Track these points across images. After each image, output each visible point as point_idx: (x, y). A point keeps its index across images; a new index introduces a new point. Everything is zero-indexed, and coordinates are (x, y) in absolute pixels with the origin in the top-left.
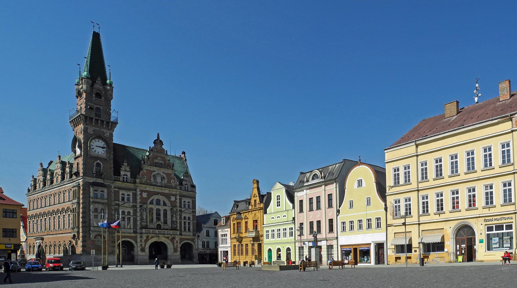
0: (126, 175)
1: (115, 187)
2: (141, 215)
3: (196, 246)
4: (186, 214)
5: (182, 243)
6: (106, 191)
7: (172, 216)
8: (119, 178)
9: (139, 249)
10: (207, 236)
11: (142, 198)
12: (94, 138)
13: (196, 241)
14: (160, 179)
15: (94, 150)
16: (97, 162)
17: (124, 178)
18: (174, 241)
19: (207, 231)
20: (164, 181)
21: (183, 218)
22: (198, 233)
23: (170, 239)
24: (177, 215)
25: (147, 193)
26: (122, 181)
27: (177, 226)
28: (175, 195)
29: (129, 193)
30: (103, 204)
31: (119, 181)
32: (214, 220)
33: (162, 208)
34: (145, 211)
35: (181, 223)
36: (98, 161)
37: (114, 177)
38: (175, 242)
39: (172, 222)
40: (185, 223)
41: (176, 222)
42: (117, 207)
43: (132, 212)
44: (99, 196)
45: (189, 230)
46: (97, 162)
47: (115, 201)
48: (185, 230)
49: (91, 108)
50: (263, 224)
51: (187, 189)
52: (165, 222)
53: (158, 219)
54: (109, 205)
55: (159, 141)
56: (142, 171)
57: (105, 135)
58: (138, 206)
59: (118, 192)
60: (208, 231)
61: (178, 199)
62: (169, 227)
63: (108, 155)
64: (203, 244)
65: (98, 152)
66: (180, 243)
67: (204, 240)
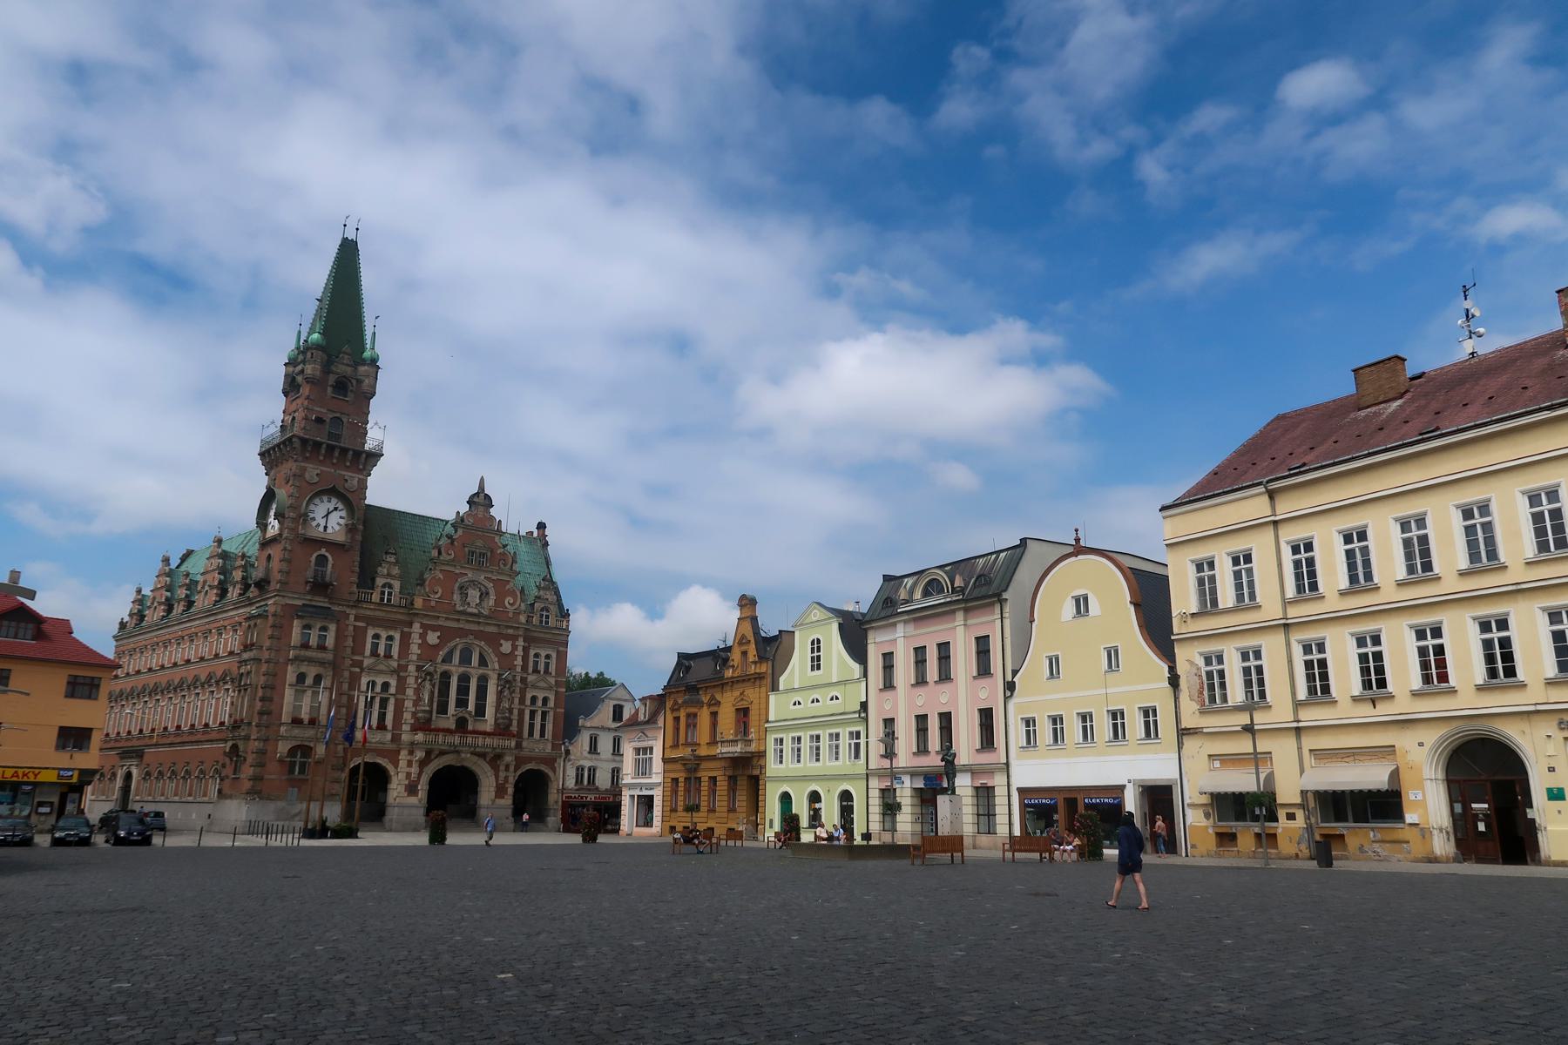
0: (390, 586)
1: (357, 618)
2: (418, 691)
3: (557, 780)
5: (519, 772)
7: (500, 694)
8: (372, 594)
9: (402, 789)
11: (424, 645)
12: (319, 494)
13: (560, 764)
14: (479, 594)
15: (314, 523)
16: (319, 553)
17: (383, 593)
18: (499, 766)
19: (591, 738)
21: (528, 702)
22: (567, 744)
23: (488, 759)
24: (514, 692)
26: (378, 601)
27: (511, 720)
28: (514, 638)
30: (322, 663)
31: (371, 602)
33: (475, 672)
34: (430, 680)
35: (521, 713)
36: (323, 551)
38: (502, 768)
40: (533, 713)
41: (511, 711)
42: (358, 670)
43: (393, 683)
44: (313, 641)
46: (319, 553)
48: (531, 734)
49: (319, 420)
52: (480, 711)
53: (462, 703)
54: (335, 666)
55: (482, 495)
57: (346, 485)
60: (596, 738)
61: (520, 648)
63: (349, 536)
64: (577, 775)
66: (515, 771)
67: (582, 763)
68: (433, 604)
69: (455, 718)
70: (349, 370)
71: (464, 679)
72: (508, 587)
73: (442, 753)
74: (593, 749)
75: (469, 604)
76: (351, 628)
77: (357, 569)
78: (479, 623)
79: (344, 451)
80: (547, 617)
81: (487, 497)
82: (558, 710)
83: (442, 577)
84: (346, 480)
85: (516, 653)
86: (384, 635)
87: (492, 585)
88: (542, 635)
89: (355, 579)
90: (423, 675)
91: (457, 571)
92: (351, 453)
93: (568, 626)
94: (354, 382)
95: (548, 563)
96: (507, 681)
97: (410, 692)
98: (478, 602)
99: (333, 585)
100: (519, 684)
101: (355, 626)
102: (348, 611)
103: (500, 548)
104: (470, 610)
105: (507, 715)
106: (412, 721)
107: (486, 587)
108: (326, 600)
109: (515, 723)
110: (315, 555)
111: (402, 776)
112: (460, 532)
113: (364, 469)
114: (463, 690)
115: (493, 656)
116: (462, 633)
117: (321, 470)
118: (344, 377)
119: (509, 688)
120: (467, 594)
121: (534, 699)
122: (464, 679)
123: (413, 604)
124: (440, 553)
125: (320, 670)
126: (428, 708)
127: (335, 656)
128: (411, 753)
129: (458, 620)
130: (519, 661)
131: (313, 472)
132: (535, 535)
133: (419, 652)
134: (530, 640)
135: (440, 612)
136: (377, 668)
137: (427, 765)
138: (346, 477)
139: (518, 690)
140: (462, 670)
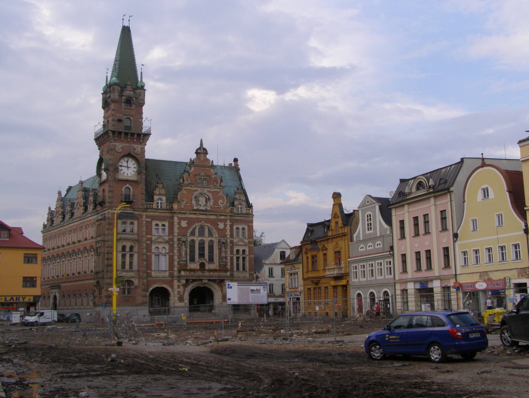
0: (161, 199)
1: (147, 217)
2: (179, 251)
4: (240, 247)
6: (136, 222)
7: (220, 249)
8: (152, 204)
9: (176, 298)
10: (269, 277)
11: (180, 227)
14: (205, 200)
16: (126, 186)
17: (158, 203)
19: (269, 269)
20: (209, 203)
21: (235, 253)
22: (257, 273)
25: (186, 221)
26: (156, 207)
27: (226, 263)
28: (225, 221)
29: (164, 223)
30: (132, 240)
31: (152, 208)
32: (281, 252)
33: (207, 239)
35: (232, 259)
36: (128, 185)
37: (146, 204)
39: (220, 257)
40: (238, 258)
41: (226, 258)
42: (149, 242)
44: (128, 230)
45: (244, 269)
46: (126, 186)
47: (147, 234)
50: (349, 258)
51: (241, 211)
52: (211, 260)
53: (202, 255)
56: (181, 192)
57: (136, 151)
58: (176, 239)
59: (151, 223)
60: (272, 269)
61: (228, 226)
62: (217, 266)
65: (128, 174)
68: (183, 207)
69: (199, 263)
70: (131, 93)
71: (202, 243)
72: (219, 195)
73: (194, 281)
74: (271, 274)
75: (200, 205)
76: (144, 222)
77: (144, 193)
78: (206, 214)
79: (133, 134)
80: (241, 208)
81: (205, 149)
82: (250, 256)
83: (185, 193)
84: (135, 149)
85: (227, 228)
86: (160, 224)
87: (211, 194)
88: (239, 218)
89: (144, 197)
90: (181, 243)
91: (193, 189)
92: (136, 135)
93: (252, 212)
94: (134, 99)
95: (240, 179)
96: (224, 243)
97: (176, 251)
98: (205, 203)
99: (134, 202)
100: (230, 244)
101: (146, 221)
102: (142, 213)
103: (214, 175)
104: (201, 208)
105: (224, 260)
106: (178, 266)
107: (208, 196)
108: (131, 209)
109: (229, 264)
110: (124, 188)
111: (176, 292)
112: (193, 169)
113: (143, 142)
114: (202, 248)
115: (214, 231)
116: (198, 220)
117: (123, 146)
118: (129, 97)
119: (224, 247)
120: (199, 200)
121: (238, 251)
122: (202, 243)
123: (173, 208)
124: (184, 181)
125: (132, 244)
126: (184, 259)
127: (138, 236)
128: (179, 281)
129: (195, 214)
130: (228, 233)
131: (119, 146)
132: (233, 165)
133: (178, 231)
134: (233, 222)
135: (186, 211)
136: (158, 241)
137: (187, 287)
138: (135, 148)
139: (229, 247)
140: (200, 238)
